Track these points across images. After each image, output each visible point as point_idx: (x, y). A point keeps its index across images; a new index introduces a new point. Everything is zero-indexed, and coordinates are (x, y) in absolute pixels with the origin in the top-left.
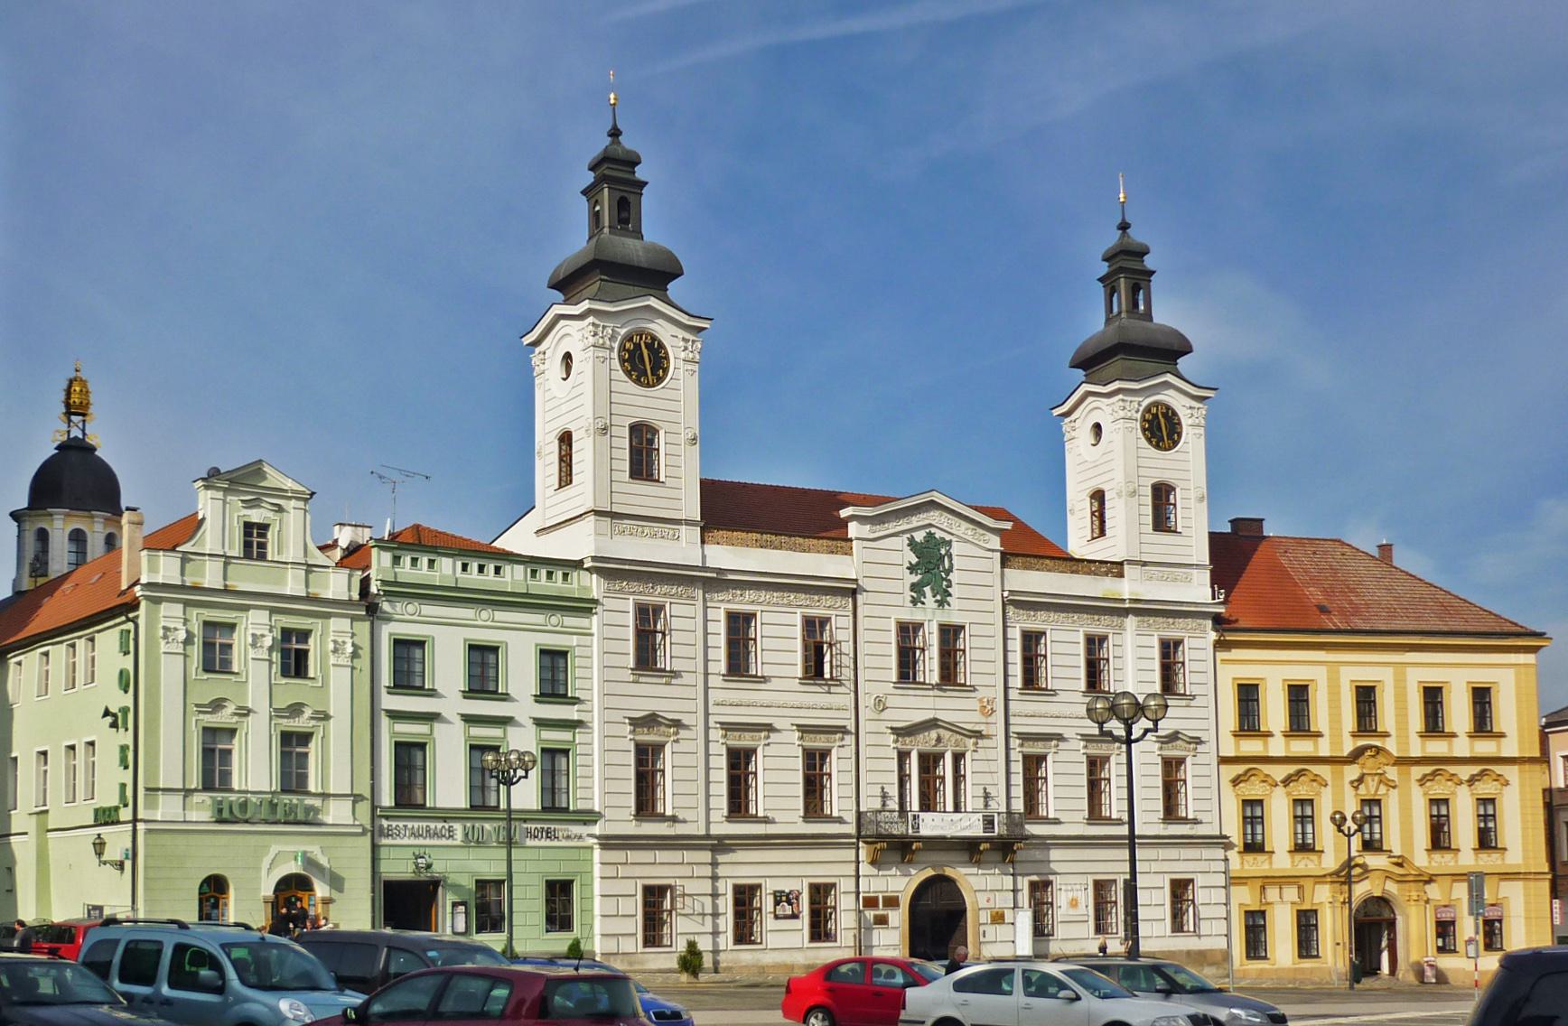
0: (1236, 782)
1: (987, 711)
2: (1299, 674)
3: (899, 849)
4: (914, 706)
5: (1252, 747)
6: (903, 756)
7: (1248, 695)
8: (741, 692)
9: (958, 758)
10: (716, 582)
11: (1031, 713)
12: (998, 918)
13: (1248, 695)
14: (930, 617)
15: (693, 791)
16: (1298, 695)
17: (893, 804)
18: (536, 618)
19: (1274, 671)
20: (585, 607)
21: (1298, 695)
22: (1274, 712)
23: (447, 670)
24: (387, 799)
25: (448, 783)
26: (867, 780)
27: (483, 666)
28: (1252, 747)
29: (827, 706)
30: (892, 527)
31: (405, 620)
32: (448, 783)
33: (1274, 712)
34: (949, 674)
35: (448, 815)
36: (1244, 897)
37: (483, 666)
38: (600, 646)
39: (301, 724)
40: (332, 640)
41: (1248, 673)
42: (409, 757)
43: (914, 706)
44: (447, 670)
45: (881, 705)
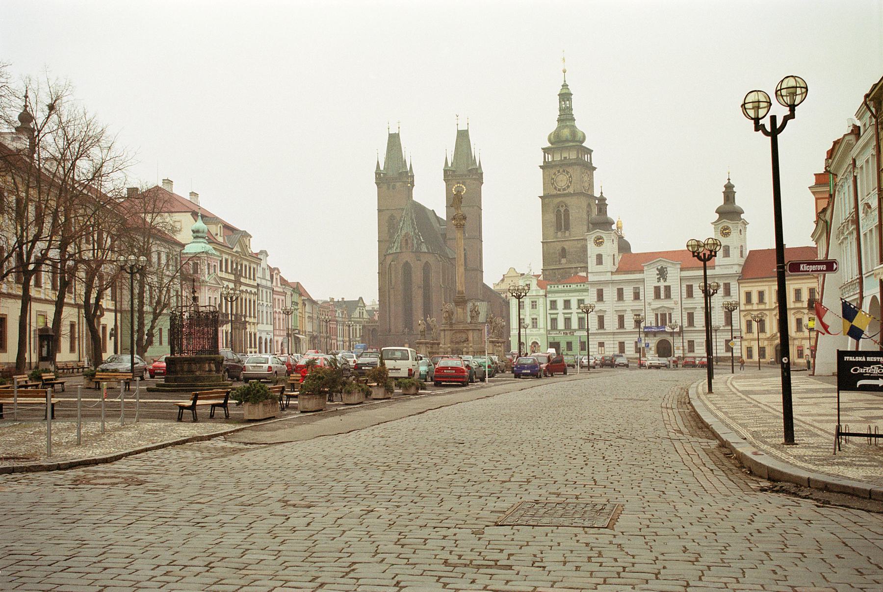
0: (744, 316)
1: (676, 303)
2: (761, 289)
3: (655, 334)
4: (657, 304)
5: (749, 307)
6: (657, 315)
7: (748, 295)
8: (621, 304)
9: (670, 314)
10: (613, 282)
11: (688, 303)
12: (678, 349)
13: (748, 295)
14: (662, 284)
15: (611, 323)
16: (761, 294)
17: (654, 324)
18: (577, 294)
19: (755, 289)
20: (586, 290)
21: (761, 294)
22: (755, 298)
23: (560, 305)
24: (549, 328)
25: (561, 325)
26: (650, 320)
27: (567, 304)
28: (749, 307)
29: (638, 305)
30: (652, 266)
31: (551, 297)
32: (561, 325)
33: (755, 298)
34: (668, 296)
35: (560, 331)
36: (745, 344)
37: (567, 304)
38: (590, 298)
39: (534, 316)
40: (541, 302)
41: (748, 289)
42: (554, 321)
43: (657, 304)
44: (560, 305)
45: (650, 304)
